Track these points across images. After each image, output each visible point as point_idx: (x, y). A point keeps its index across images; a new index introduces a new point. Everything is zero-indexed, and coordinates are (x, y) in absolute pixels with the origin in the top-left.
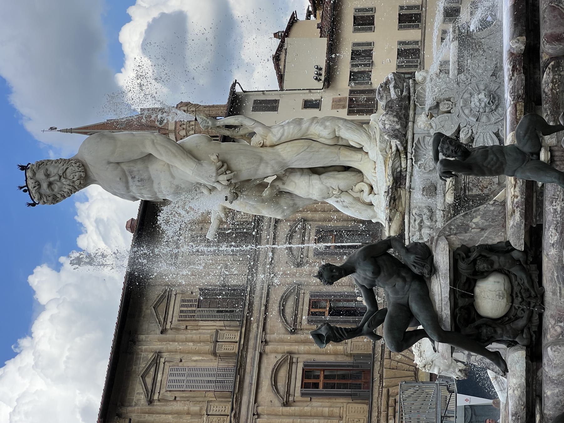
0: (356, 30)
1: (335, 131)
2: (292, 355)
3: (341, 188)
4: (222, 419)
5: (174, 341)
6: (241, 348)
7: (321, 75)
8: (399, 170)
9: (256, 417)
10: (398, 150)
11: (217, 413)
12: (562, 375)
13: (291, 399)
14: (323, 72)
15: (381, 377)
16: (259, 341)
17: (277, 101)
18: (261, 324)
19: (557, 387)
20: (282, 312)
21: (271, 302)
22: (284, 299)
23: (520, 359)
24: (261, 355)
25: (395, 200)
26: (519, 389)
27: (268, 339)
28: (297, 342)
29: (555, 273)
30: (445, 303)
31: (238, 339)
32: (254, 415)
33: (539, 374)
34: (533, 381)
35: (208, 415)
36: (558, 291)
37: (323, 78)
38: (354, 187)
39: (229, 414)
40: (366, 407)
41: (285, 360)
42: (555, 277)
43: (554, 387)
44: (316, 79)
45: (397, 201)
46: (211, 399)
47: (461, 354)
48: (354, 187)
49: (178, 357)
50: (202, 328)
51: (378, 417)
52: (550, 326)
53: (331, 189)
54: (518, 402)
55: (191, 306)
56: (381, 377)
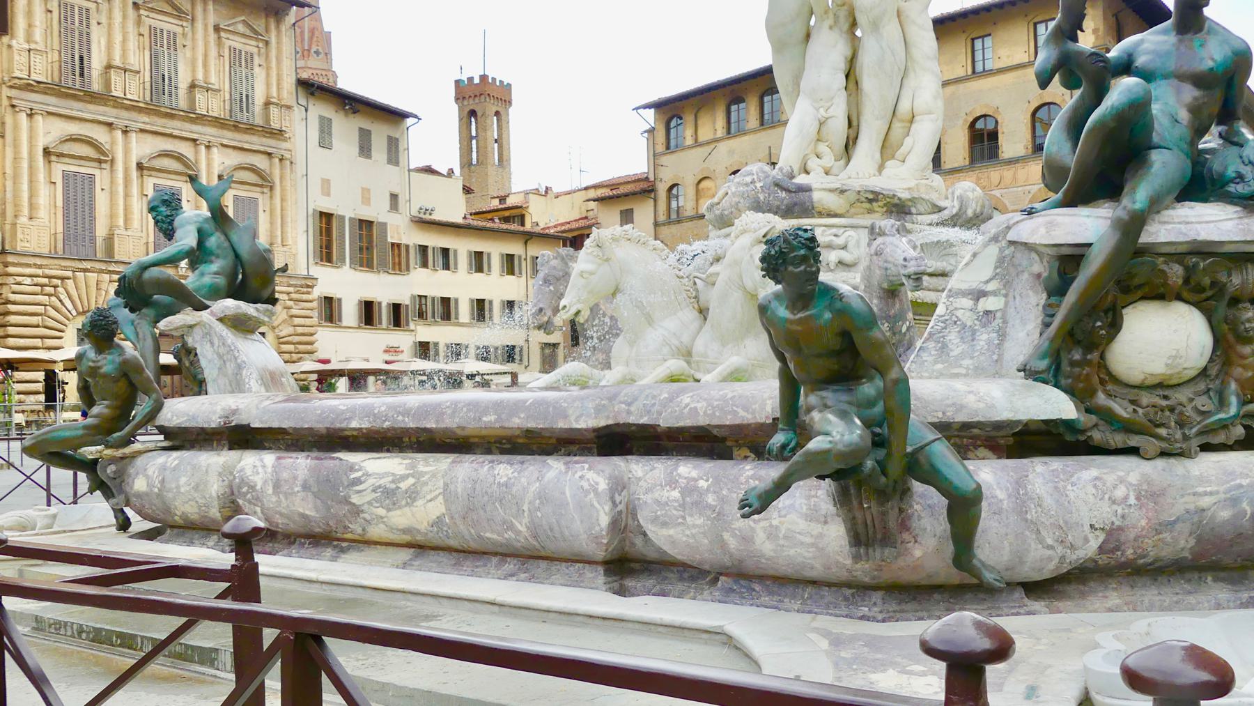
0: (470, 253)
1: (930, 113)
2: (109, 162)
3: (829, 120)
4: (24, 68)
5: (125, 17)
6: (119, 100)
7: (425, 214)
8: (914, 210)
9: (29, 112)
10: (940, 210)
11: (32, 63)
12: (1040, 506)
13: (53, 158)
14: (427, 217)
15: (85, 270)
16: (127, 123)
17: (397, 163)
18: (148, 127)
19: (1009, 496)
20: (166, 154)
21: (176, 142)
22: (179, 158)
23: (1055, 405)
24: (110, 125)
25: (870, 201)
26: (982, 405)
27: (129, 134)
28: (126, 170)
29: (1248, 481)
30: (1184, 231)
31: (129, 96)
32: (31, 109)
33: (982, 452)
34: (971, 438)
35: (29, 51)
36: (1209, 489)
37: (422, 215)
38: (827, 144)
39: (32, 78)
40: (45, 251)
41: (103, 153)
42: (1238, 481)
43: (1007, 489)
44: (421, 209)
45: (867, 205)
46: (49, 56)
47: (988, 273)
48: (827, 144)
49: (104, 20)
50: (141, 53)
51: (35, 265)
52: (1122, 474)
53: (830, 104)
54: (949, 402)
55: (169, 43)
56: (85, 270)
